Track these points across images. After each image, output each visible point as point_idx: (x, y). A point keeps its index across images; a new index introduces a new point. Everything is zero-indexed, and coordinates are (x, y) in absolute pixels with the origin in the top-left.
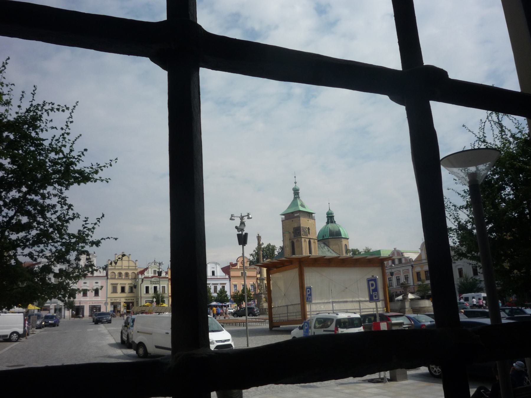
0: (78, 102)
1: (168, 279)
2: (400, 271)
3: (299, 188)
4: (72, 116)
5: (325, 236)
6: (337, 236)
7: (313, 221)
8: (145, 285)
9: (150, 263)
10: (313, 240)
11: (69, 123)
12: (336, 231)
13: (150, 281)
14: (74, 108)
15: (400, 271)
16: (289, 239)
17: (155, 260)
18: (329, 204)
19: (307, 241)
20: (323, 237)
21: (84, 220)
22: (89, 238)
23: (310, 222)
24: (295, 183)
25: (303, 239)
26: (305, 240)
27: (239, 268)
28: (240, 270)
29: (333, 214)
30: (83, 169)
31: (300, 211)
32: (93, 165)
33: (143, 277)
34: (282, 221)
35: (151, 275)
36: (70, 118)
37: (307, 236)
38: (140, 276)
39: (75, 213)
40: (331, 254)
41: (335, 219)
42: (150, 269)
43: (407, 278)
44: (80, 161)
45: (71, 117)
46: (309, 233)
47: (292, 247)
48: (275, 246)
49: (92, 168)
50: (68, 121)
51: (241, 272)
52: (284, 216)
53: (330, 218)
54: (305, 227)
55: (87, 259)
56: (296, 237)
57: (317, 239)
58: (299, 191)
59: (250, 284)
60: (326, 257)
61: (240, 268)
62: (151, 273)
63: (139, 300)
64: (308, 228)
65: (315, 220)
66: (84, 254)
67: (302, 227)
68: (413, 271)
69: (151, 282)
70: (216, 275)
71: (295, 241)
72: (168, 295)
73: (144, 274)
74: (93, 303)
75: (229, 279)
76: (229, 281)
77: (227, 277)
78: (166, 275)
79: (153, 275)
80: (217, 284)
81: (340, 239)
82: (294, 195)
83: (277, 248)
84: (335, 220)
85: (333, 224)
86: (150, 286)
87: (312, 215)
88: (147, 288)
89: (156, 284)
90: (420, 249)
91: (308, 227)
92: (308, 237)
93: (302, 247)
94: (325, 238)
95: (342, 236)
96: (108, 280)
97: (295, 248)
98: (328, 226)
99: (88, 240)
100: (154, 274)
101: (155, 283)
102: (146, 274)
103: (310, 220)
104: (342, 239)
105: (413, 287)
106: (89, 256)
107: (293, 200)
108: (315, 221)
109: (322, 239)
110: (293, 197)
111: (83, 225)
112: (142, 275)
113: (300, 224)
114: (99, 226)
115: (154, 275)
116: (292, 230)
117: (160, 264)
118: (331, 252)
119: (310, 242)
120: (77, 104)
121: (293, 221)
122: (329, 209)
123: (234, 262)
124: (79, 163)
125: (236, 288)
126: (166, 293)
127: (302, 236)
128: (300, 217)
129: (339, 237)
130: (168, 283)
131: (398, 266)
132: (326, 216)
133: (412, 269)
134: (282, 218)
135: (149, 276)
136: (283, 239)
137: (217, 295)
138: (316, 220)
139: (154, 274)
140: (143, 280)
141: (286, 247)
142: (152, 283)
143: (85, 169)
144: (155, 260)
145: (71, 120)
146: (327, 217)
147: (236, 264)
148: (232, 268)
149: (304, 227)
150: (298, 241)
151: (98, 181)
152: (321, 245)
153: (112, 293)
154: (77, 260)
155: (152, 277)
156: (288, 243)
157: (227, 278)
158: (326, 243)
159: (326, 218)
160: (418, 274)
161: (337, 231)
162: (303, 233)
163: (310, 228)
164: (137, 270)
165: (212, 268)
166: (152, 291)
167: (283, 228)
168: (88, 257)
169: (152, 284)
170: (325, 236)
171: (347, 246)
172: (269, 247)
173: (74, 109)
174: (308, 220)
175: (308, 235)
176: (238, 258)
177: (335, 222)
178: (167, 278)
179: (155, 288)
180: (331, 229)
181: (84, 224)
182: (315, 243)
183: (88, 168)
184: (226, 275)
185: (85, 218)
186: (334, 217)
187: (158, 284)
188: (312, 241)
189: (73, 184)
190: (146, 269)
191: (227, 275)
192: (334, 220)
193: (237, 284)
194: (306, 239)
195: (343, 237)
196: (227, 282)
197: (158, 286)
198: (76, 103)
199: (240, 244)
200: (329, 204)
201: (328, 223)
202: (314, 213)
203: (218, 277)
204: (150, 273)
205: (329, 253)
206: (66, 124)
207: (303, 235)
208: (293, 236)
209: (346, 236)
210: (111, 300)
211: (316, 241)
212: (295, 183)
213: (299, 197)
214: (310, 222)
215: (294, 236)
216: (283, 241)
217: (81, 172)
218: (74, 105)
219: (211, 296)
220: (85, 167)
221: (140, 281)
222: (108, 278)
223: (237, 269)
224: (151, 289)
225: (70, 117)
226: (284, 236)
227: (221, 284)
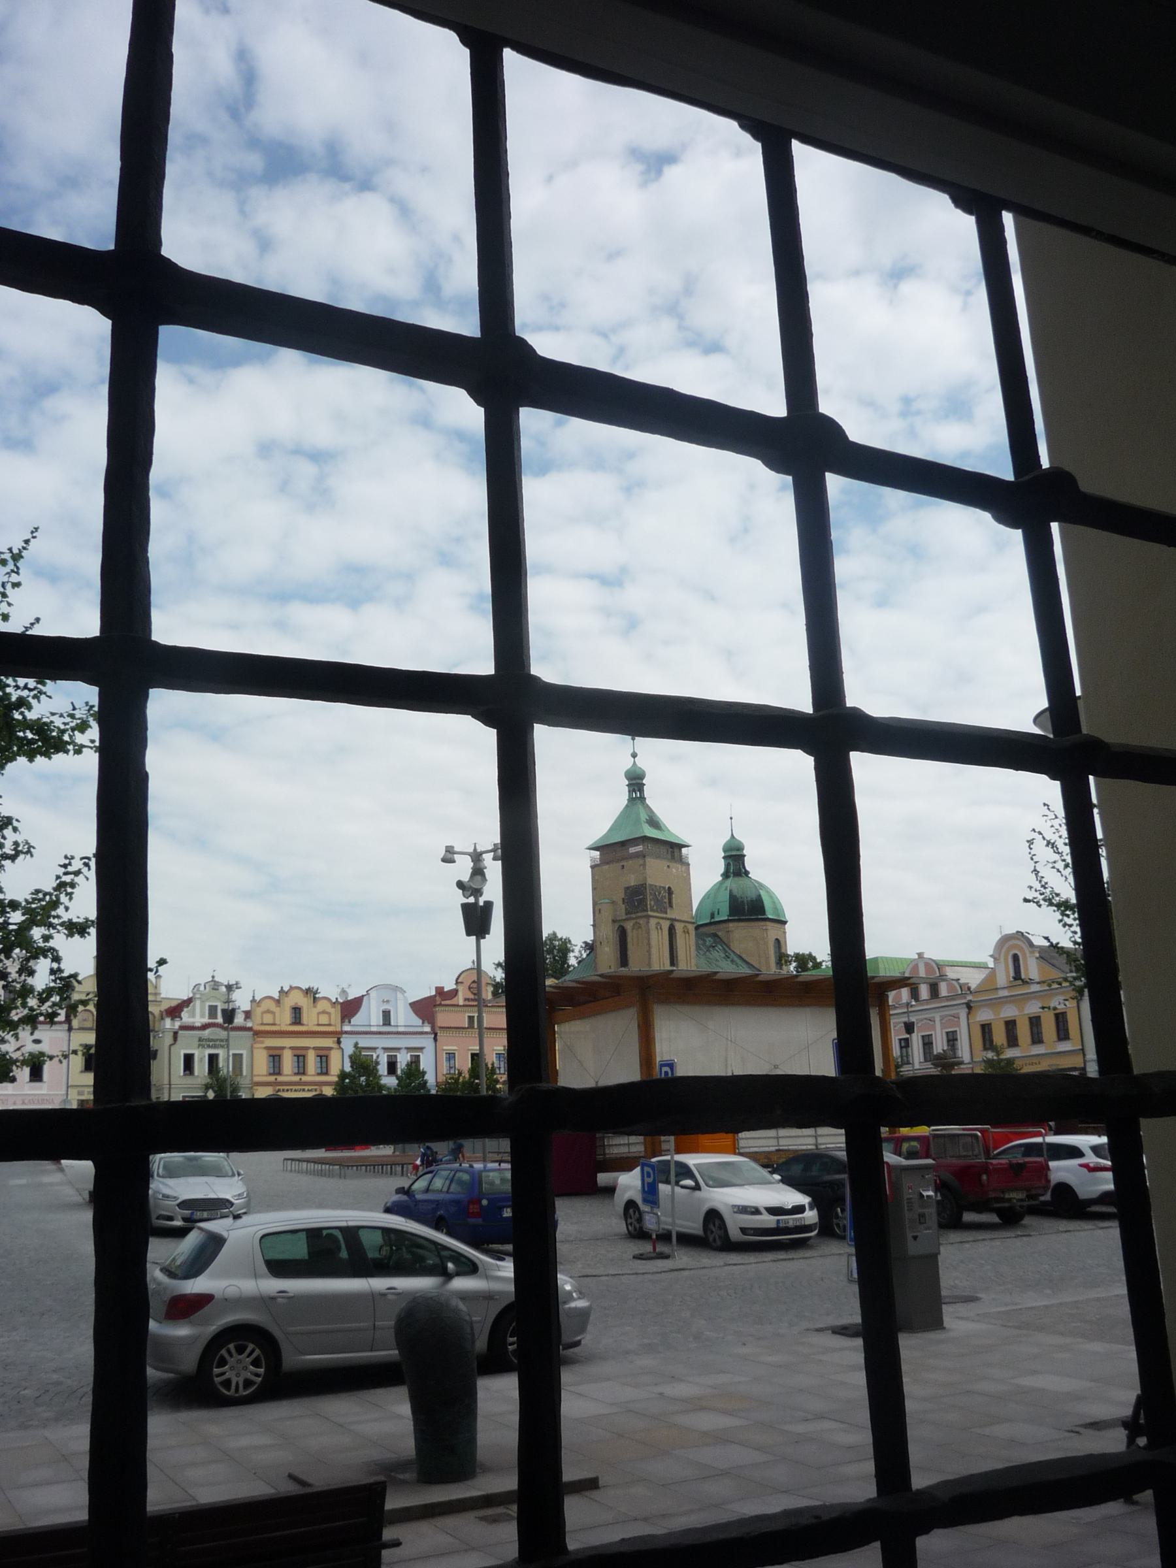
0: (36, 529)
1: (251, 1033)
2: (932, 1020)
3: (644, 771)
4: (18, 568)
5: (718, 914)
6: (751, 915)
7: (684, 868)
8: (183, 1049)
9: (199, 984)
10: (683, 925)
11: (9, 586)
12: (749, 899)
13: (197, 1040)
14: (25, 545)
15: (934, 1021)
16: (610, 919)
17: (213, 977)
18: (731, 818)
19: (663, 928)
20: (712, 916)
21: (62, 864)
22: (60, 911)
23: (674, 870)
24: (634, 755)
25: (653, 922)
26: (658, 923)
27: (461, 1002)
28: (465, 1008)
29: (743, 849)
30: (48, 718)
31: (645, 839)
32: (77, 707)
33: (177, 1024)
34: (592, 867)
35: (199, 1020)
36: (13, 574)
37: (666, 913)
38: (168, 1023)
39: (20, 841)
40: (734, 966)
41: (749, 864)
42: (198, 1003)
43: (952, 1039)
44: (43, 697)
45: (15, 570)
46: (671, 905)
47: (621, 946)
48: (570, 941)
49: (72, 716)
50: (8, 582)
51: (469, 1017)
52: (598, 853)
53: (735, 860)
54: (660, 887)
55: (53, 972)
56: (634, 916)
57: (693, 921)
58: (644, 782)
59: (493, 1050)
60: (718, 975)
61: (467, 1003)
62: (202, 1016)
63: (163, 1093)
64: (669, 888)
65: (689, 865)
66: (45, 957)
67: (651, 885)
68: (970, 1021)
69: (200, 1040)
70: (392, 1023)
71: (629, 926)
72: (252, 1080)
73: (181, 1019)
74: (26, 1101)
75: (433, 1036)
76: (432, 1039)
77: (427, 1029)
78: (245, 1020)
79: (206, 1020)
80: (398, 1049)
81: (762, 923)
82: (629, 791)
83: (576, 946)
84: (747, 869)
85: (740, 878)
86: (197, 1053)
87: (680, 851)
88: (189, 1060)
89: (215, 1047)
90: (991, 956)
91: (667, 887)
92: (668, 916)
93: (649, 944)
94: (717, 919)
95: (767, 913)
96: (72, 1034)
97: (630, 946)
98: (725, 885)
99: (58, 917)
100: (210, 1018)
101: (211, 1044)
102: (186, 1017)
103: (671, 864)
104: (768, 923)
105: (971, 1066)
106: (59, 964)
107: (627, 806)
108: (688, 869)
109: (708, 921)
110: (627, 798)
111: (58, 877)
112: (172, 1019)
113: (645, 878)
114: (87, 879)
115: (211, 1021)
116: (620, 895)
117: (229, 988)
118: (732, 961)
119: (672, 930)
120: (34, 535)
121: (623, 866)
122: (732, 835)
123: (449, 986)
124: (39, 701)
125: (452, 1062)
126: (244, 1074)
127: (650, 913)
128: (644, 857)
129: (760, 917)
130: (252, 1047)
131: (927, 1004)
132: (723, 855)
133: (969, 1014)
134: (592, 859)
135: (194, 1023)
136: (594, 921)
137: (397, 1082)
138: (691, 866)
139: (210, 1018)
140: (175, 1034)
141: (601, 943)
142: (204, 1043)
143: (52, 718)
144: (213, 977)
145: (14, 578)
146: (724, 858)
147: (454, 993)
148: (443, 1003)
149: (656, 886)
150: (637, 926)
151: (84, 750)
152: (705, 941)
153: (82, 1072)
154: (24, 974)
155: (204, 1027)
156: (609, 932)
157: (426, 1033)
158: (720, 934)
159: (723, 860)
160: (986, 1029)
161: (752, 901)
162: (652, 903)
163: (673, 889)
164: (160, 1005)
165: (383, 1001)
166: (201, 1068)
167: (594, 889)
168: (55, 965)
169: (203, 1047)
170: (718, 914)
171: (782, 943)
172: (552, 943)
173: (24, 548)
174: (668, 866)
175: (668, 910)
176: (461, 974)
177: (747, 873)
178: (250, 1029)
179: (213, 1059)
180: (735, 892)
181: (61, 875)
182: (686, 932)
183: (61, 716)
184: (423, 1023)
185: (66, 857)
186: (746, 858)
187: (222, 1047)
188: (679, 927)
189: (16, 760)
190: (187, 1002)
191: (426, 1024)
192: (744, 867)
193: (454, 1050)
194: (662, 921)
195: (770, 917)
196: (427, 1042)
197: (221, 1052)
198: (32, 532)
199: (469, 934)
200: (731, 818)
201: (726, 875)
202: (688, 846)
203: (401, 1029)
204: (196, 1016)
205: (729, 962)
206: (2, 590)
207: (652, 910)
208: (624, 911)
209: (779, 916)
210: (79, 1093)
211: (691, 928)
212: (634, 755)
213: (642, 799)
214: (674, 870)
216: (594, 926)
217: (41, 728)
218: (26, 538)
219: (378, 1083)
220: (53, 714)
221: (168, 1039)
222: (70, 1029)
223: (458, 1006)
224: (201, 1060)
225: (13, 571)
226: (597, 912)
227: (409, 1049)
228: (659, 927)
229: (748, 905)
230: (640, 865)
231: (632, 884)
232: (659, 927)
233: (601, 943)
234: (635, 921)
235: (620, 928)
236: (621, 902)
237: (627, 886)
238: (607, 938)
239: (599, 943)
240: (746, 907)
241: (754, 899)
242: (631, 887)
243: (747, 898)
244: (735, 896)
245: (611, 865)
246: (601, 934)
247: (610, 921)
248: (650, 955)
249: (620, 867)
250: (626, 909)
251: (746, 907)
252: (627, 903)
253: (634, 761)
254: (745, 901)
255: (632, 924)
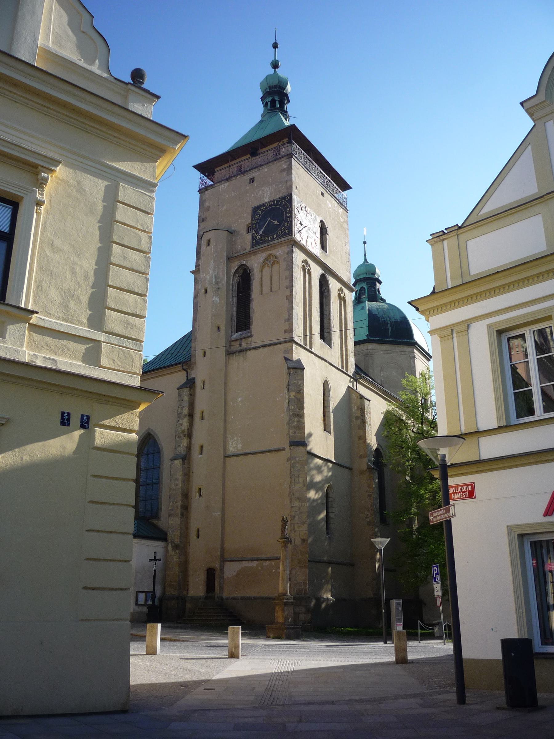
34: (201, 191)
47: (238, 298)
82: (265, 105)
97: (255, 294)
103: (327, 195)
107: (261, 122)
121: (252, 180)
122: (366, 260)
136: (198, 265)
141: (206, 291)
161: (396, 322)
180: (375, 312)
215: (255, 242)
228: (306, 271)
229: (391, 326)
230: (283, 171)
231: (266, 200)
232: (306, 271)
233: (206, 291)
234: (268, 253)
235: (241, 271)
236: (244, 231)
237: (256, 204)
238: (217, 283)
239: (203, 291)
240: (390, 328)
241: (399, 321)
242: (263, 205)
243: (390, 319)
244: (376, 315)
245: (234, 181)
246: (208, 277)
247: (225, 258)
248: (291, 303)
249: (248, 181)
250: (253, 238)
251: (390, 328)
252: (255, 228)
253: (275, 71)
254: (389, 322)
255: (262, 259)
